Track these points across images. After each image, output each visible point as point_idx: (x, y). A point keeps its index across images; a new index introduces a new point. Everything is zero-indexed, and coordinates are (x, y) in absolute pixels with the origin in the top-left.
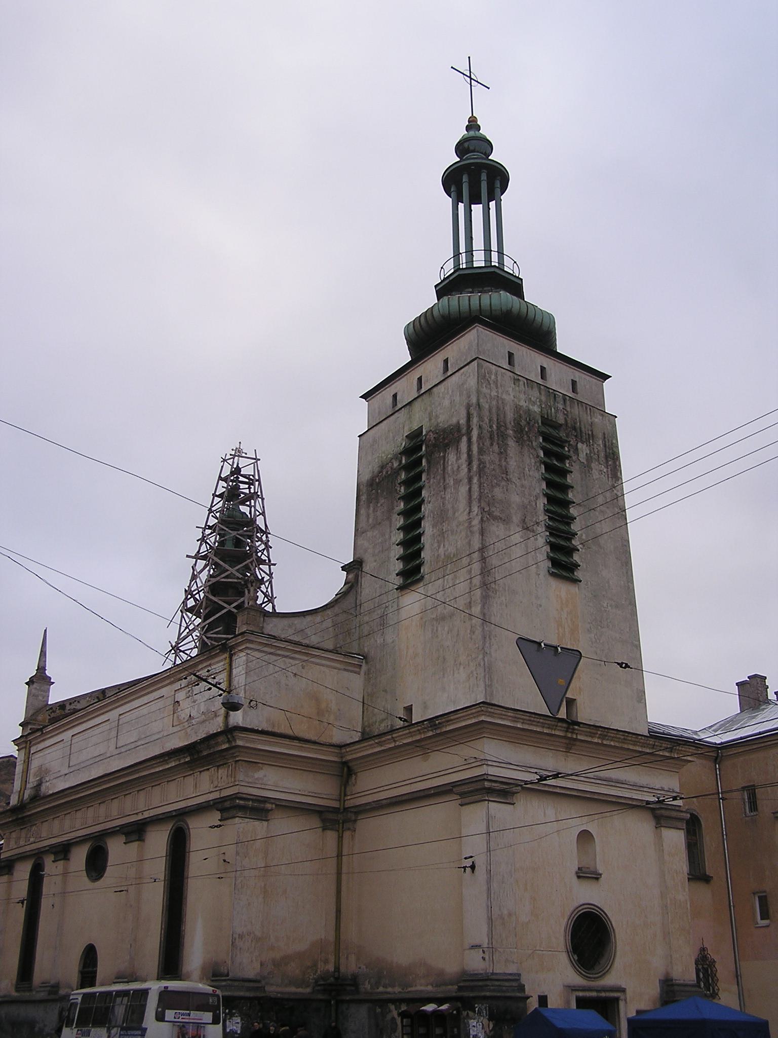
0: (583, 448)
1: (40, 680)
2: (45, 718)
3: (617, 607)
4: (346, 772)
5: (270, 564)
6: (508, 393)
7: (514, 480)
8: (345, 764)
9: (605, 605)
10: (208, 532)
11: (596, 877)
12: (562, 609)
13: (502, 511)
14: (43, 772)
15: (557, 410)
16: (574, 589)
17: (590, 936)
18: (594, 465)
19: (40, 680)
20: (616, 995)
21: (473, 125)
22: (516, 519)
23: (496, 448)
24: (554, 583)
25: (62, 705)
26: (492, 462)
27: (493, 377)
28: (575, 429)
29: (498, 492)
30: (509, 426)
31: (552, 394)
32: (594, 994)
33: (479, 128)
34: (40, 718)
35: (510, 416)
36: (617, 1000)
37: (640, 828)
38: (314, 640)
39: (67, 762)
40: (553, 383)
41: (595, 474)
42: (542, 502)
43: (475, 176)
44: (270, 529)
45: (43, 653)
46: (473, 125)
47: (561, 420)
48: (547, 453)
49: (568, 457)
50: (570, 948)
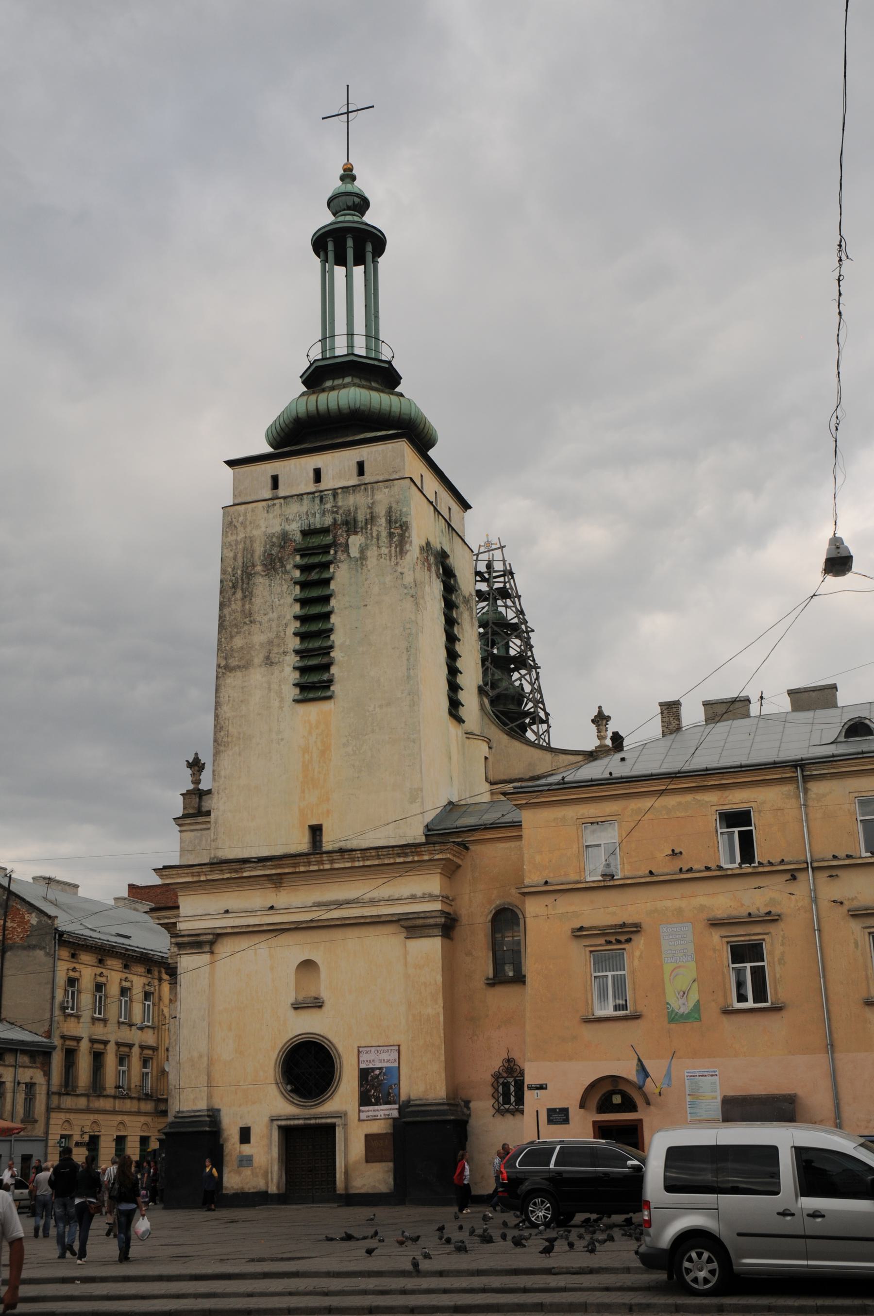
3: (388, 704)
6: (258, 527)
7: (258, 618)
9: (371, 709)
11: (317, 1004)
12: (310, 733)
15: (323, 514)
17: (307, 1066)
20: (329, 1121)
21: (348, 175)
22: (258, 659)
23: (239, 595)
24: (302, 709)
27: (241, 519)
30: (257, 562)
32: (301, 1122)
33: (353, 178)
35: (259, 550)
36: (332, 1128)
37: (387, 944)
43: (349, 241)
46: (348, 175)
47: (328, 521)
48: (304, 569)
50: (279, 1078)
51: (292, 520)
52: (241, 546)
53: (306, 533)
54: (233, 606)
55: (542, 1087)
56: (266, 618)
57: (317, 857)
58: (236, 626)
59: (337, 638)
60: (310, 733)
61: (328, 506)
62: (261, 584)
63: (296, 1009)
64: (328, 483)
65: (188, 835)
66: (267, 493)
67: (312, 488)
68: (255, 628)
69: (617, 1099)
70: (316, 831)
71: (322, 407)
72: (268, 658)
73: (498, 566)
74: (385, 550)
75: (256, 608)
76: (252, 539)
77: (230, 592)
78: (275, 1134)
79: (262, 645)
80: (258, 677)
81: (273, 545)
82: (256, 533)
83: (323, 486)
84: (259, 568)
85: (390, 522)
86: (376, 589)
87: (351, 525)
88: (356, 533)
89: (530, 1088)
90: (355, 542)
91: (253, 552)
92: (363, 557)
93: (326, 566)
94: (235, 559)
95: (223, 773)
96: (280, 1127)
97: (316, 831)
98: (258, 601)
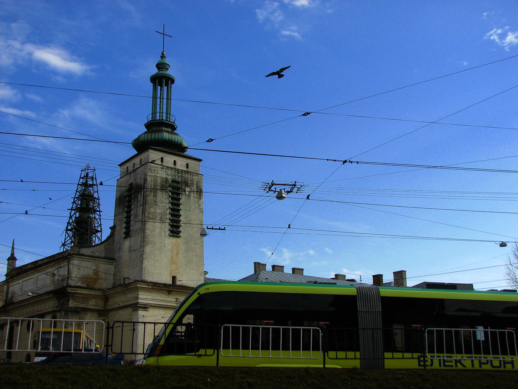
0: (187, 189)
1: (12, 259)
2: (15, 273)
3: (196, 244)
4: (106, 298)
5: (100, 211)
8: (106, 296)
10: (76, 199)
13: (153, 216)
14: (14, 293)
15: (178, 176)
16: (179, 240)
18: (192, 194)
19: (12, 259)
21: (163, 56)
22: (158, 218)
23: (152, 194)
25: (21, 268)
26: (151, 199)
28: (185, 183)
29: (152, 210)
31: (178, 170)
34: (12, 273)
35: (159, 181)
38: (98, 254)
39: (24, 288)
40: (178, 167)
41: (192, 198)
42: (169, 211)
44: (100, 197)
45: (13, 248)
47: (180, 180)
49: (181, 194)
51: (170, 176)
52: (153, 178)
53: (173, 181)
56: (160, 205)
58: (151, 204)
59: (182, 218)
61: (180, 175)
62: (159, 193)
67: (173, 166)
68: (157, 207)
70: (174, 278)
71: (170, 138)
72: (161, 218)
73: (90, 175)
74: (195, 195)
81: (163, 181)
84: (159, 188)
85: (197, 187)
86: (193, 207)
87: (187, 185)
90: (187, 189)
91: (157, 181)
92: (189, 196)
93: (179, 194)
94: (151, 181)
97: (174, 278)
98: (158, 198)
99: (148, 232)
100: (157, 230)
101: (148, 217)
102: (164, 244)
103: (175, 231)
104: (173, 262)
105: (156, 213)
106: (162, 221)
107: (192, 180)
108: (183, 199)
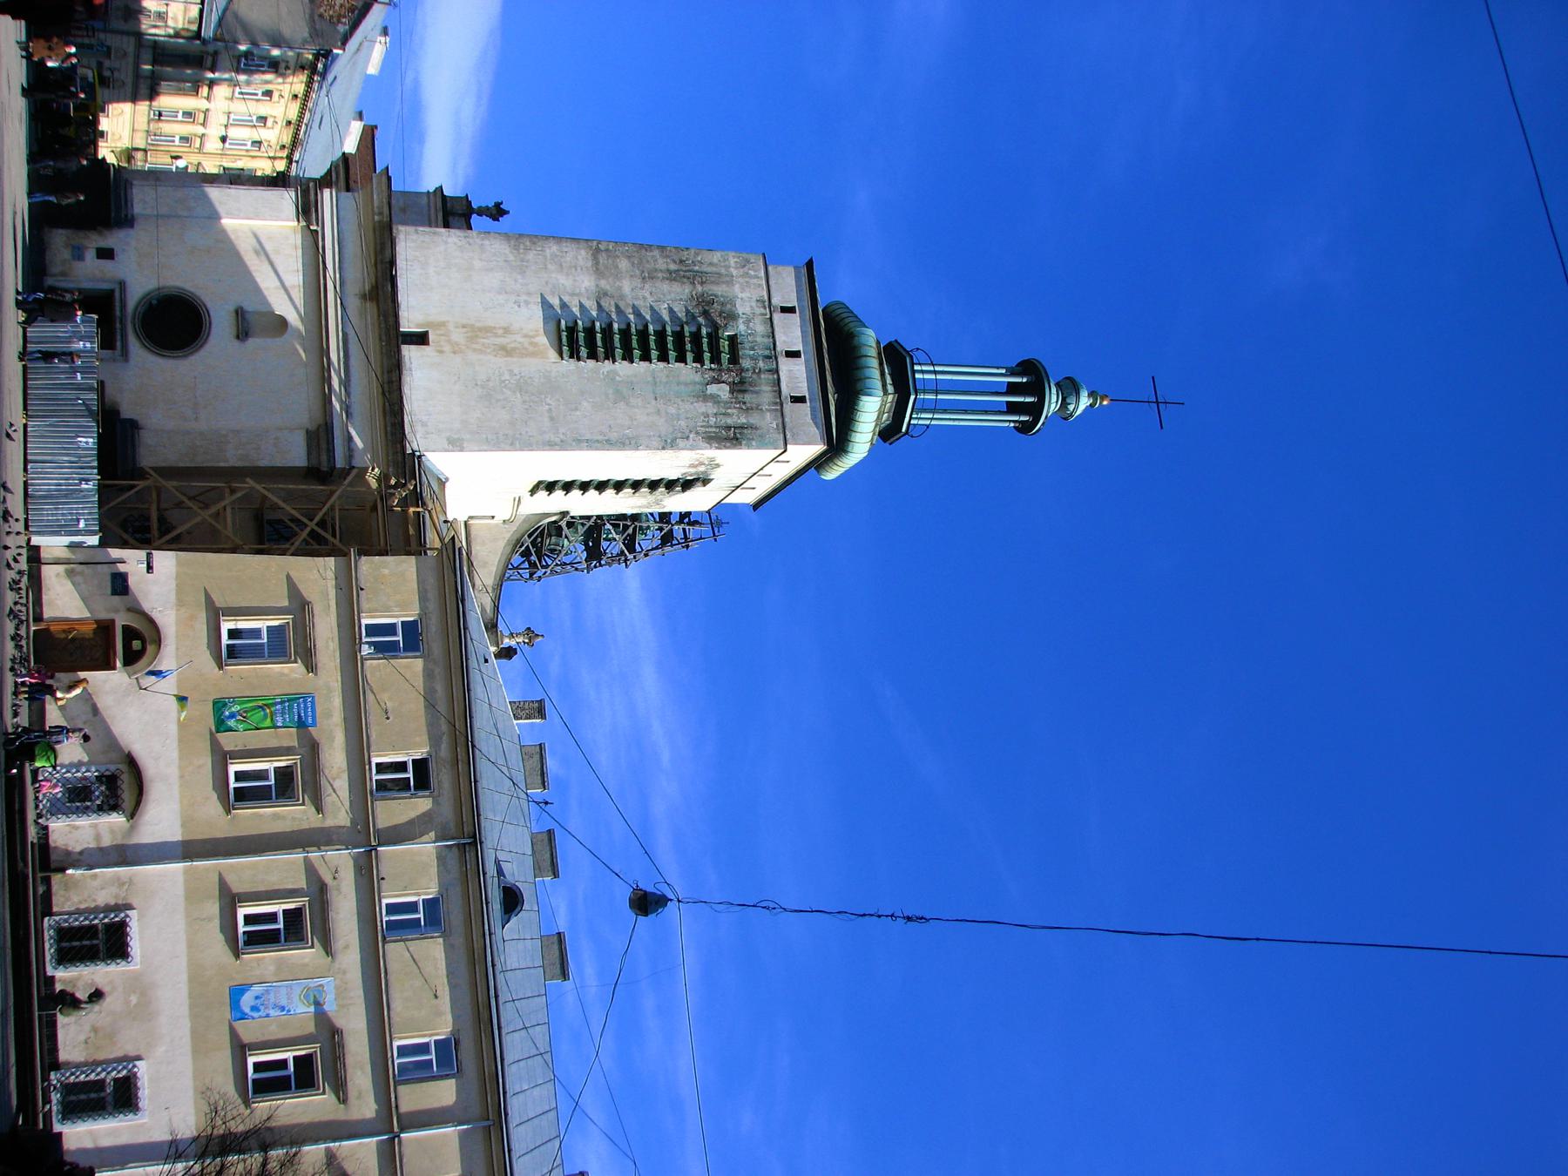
3: (552, 419)
6: (743, 291)
12: (526, 336)
15: (752, 358)
18: (710, 408)
20: (118, 344)
23: (673, 267)
29: (624, 264)
30: (707, 288)
35: (719, 290)
47: (746, 363)
50: (166, 292)
51: (747, 323)
52: (723, 271)
54: (660, 261)
55: (150, 568)
57: (392, 340)
58: (640, 262)
59: (622, 367)
60: (526, 336)
61: (761, 364)
63: (237, 312)
64: (786, 366)
65: (425, 200)
66: (777, 301)
67: (781, 347)
68: (638, 282)
69: (136, 645)
70: (421, 339)
72: (605, 294)
75: (658, 284)
76: (730, 283)
77: (676, 258)
78: (105, 286)
79: (620, 288)
80: (587, 284)
82: (737, 288)
83: (783, 361)
84: (700, 288)
86: (672, 410)
87: (739, 387)
88: (732, 392)
89: (149, 556)
90: (723, 391)
92: (706, 398)
93: (699, 359)
94: (711, 264)
95: (487, 242)
96: (113, 291)
97: (421, 339)
98: (665, 286)
99: (552, 248)
100: (564, 281)
101: (598, 250)
102: (527, 303)
103: (582, 338)
104: (476, 332)
105: (618, 276)
106: (600, 295)
107: (758, 408)
108: (687, 372)
